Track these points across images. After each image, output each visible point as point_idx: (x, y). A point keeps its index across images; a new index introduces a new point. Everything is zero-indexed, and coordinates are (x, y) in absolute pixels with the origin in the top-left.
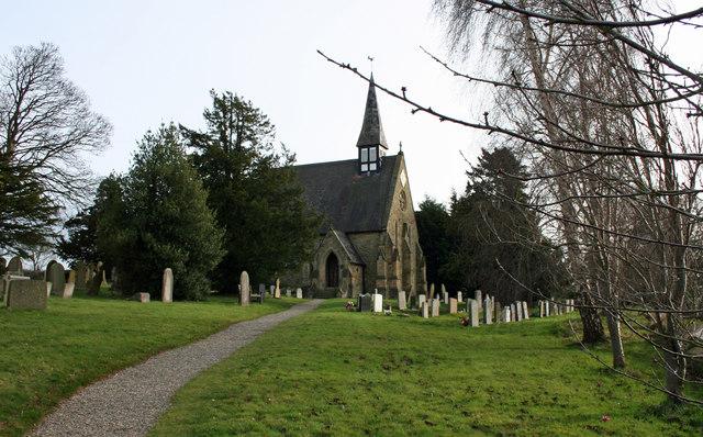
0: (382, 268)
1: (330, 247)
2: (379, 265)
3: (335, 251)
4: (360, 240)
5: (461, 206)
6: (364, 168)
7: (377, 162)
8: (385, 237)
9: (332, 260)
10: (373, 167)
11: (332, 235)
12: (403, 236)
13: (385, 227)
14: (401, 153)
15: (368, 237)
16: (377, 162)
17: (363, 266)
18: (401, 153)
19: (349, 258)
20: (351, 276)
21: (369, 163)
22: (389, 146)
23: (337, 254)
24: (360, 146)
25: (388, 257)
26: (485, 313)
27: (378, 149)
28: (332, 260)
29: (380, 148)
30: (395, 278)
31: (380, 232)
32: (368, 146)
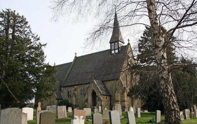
0: (118, 97)
1: (92, 87)
2: (116, 95)
3: (95, 89)
4: (109, 85)
5: (51, 70)
6: (113, 52)
7: (118, 49)
8: (119, 82)
9: (94, 94)
10: (117, 51)
11: (93, 82)
12: (131, 81)
13: (119, 77)
14: (129, 44)
15: (112, 82)
16: (118, 49)
17: (110, 96)
18: (129, 44)
19: (100, 92)
20: (101, 101)
21: (115, 50)
22: (125, 42)
23: (96, 93)
24: (111, 43)
25: (121, 91)
26: (137, 112)
27: (118, 43)
28: (94, 94)
29: (120, 43)
30: (124, 101)
31: (117, 79)
32: (114, 42)
